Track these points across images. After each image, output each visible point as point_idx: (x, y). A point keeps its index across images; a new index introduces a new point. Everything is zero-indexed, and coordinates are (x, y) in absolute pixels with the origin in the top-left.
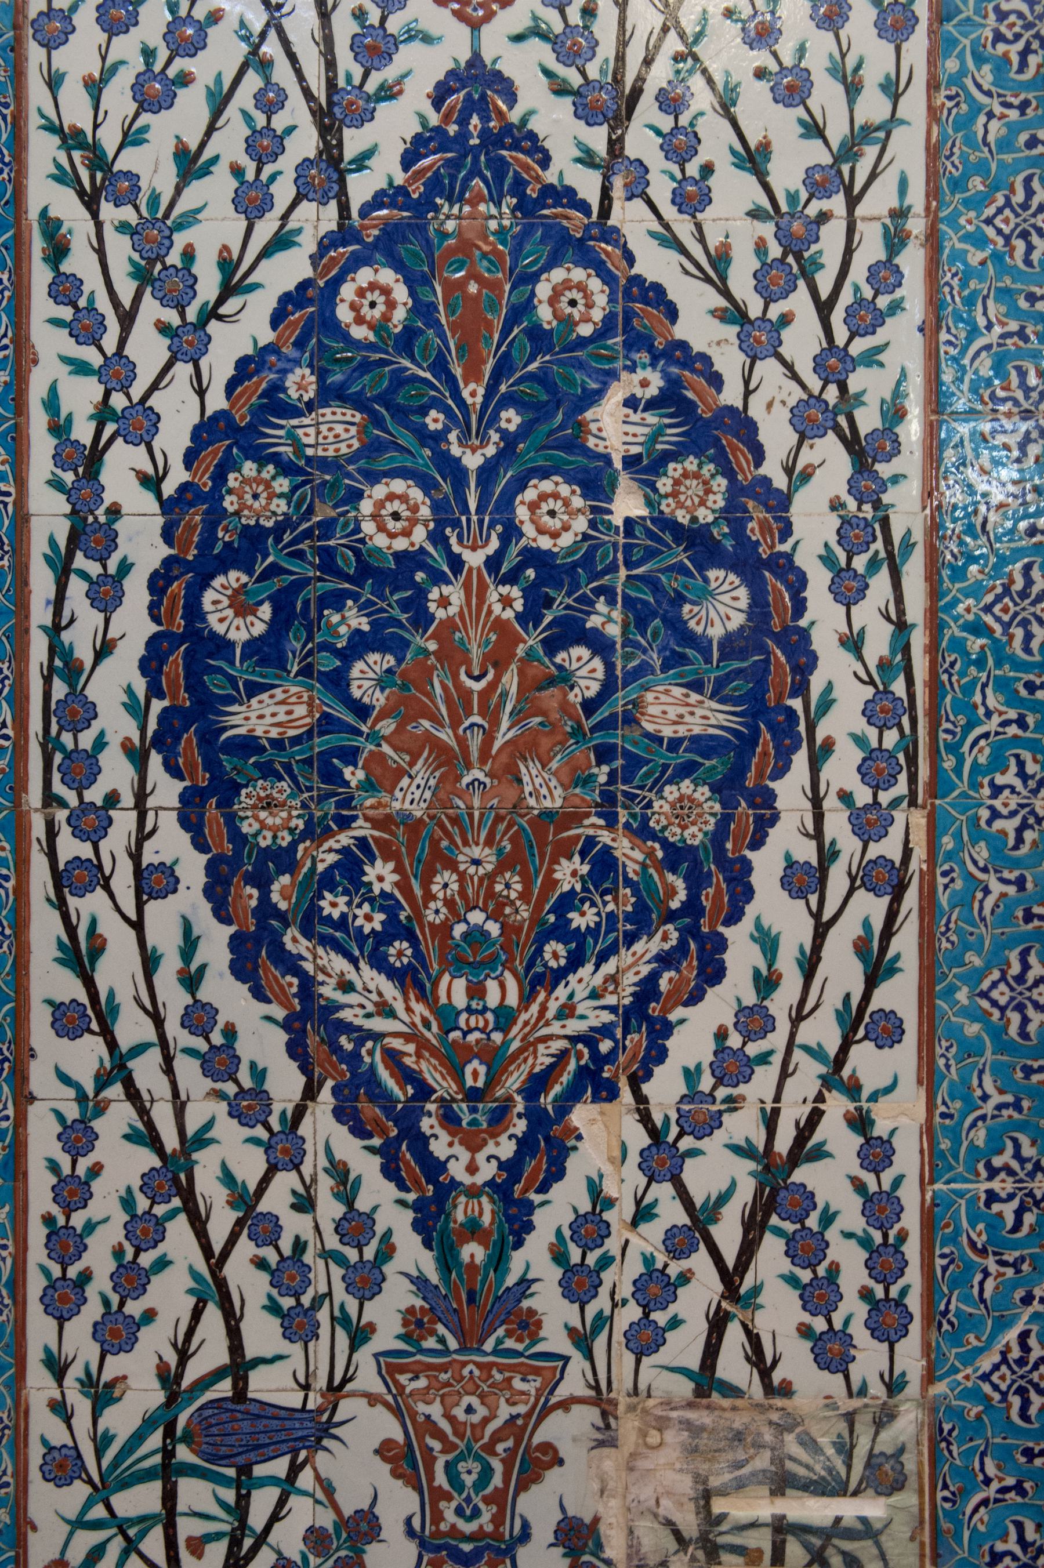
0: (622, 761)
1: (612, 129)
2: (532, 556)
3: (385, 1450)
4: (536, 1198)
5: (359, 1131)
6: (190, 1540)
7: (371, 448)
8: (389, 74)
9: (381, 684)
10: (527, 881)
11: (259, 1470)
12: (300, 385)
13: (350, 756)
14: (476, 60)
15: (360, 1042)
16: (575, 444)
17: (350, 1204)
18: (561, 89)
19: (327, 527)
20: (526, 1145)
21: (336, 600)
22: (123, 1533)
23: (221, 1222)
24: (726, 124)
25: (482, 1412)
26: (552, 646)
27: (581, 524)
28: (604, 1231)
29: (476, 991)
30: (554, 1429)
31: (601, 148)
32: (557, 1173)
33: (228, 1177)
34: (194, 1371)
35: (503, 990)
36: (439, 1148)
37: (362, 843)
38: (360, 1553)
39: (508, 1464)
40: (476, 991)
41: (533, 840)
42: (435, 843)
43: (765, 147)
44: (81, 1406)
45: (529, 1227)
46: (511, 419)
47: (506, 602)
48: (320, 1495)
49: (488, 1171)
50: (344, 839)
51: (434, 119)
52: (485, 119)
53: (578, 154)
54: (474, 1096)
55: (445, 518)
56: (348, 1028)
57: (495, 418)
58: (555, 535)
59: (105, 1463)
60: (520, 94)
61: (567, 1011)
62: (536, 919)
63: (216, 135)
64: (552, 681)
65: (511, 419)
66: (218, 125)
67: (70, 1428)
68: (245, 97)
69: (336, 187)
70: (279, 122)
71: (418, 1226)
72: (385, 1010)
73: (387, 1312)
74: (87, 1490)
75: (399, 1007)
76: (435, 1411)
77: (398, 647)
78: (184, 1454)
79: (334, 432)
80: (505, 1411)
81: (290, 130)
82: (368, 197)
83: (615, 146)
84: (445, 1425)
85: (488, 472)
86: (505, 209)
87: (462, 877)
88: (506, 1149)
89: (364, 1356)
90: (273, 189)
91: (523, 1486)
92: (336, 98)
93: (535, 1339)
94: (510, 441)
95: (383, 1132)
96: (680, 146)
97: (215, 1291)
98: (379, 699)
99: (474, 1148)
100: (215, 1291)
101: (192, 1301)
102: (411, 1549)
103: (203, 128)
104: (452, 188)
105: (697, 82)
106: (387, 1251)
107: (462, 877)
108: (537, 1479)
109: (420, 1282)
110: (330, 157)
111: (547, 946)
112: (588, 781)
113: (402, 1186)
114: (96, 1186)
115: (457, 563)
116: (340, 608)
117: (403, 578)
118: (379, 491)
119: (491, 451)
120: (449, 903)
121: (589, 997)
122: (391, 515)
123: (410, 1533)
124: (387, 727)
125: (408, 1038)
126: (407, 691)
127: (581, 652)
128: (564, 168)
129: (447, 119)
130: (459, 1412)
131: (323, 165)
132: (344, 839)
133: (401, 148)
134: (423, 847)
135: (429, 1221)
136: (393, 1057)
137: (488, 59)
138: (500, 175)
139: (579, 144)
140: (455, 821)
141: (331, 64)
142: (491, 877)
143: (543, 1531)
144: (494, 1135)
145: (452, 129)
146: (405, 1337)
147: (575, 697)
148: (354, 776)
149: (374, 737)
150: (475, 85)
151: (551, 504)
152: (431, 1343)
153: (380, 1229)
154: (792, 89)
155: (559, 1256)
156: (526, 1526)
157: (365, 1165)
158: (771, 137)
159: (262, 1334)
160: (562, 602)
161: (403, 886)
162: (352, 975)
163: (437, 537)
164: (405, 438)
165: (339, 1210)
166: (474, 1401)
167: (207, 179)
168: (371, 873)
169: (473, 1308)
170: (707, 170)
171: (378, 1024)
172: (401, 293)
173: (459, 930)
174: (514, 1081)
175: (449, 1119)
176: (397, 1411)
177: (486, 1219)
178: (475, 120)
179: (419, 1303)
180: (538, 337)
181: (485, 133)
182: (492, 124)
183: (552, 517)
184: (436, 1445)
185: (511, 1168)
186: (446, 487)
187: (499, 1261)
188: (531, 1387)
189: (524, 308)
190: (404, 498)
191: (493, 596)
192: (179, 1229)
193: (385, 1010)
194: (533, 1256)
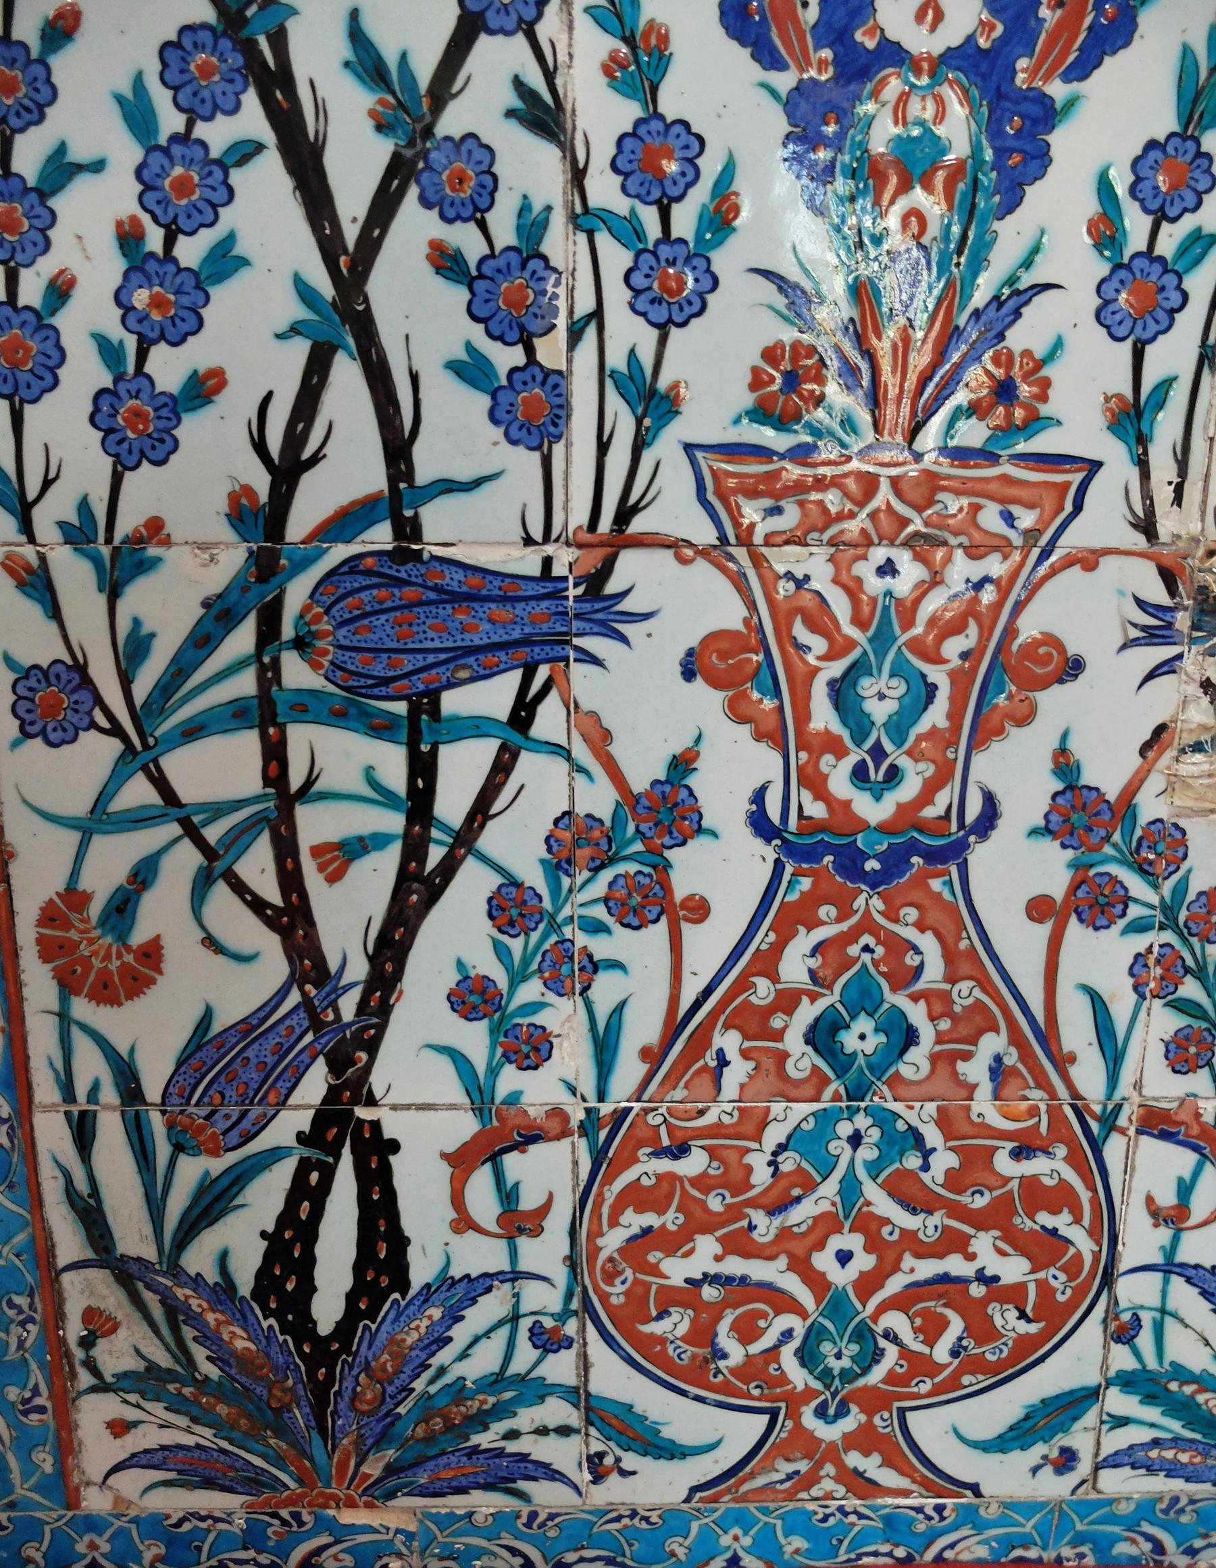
6: (317, 851)
11: (454, 702)
22: (192, 832)
23: (356, 162)
33: (368, 64)
34: (312, 503)
38: (663, 868)
44: (74, 575)
48: (581, 752)
59: (142, 689)
67: (55, 612)
74: (114, 746)
78: (297, 673)
91: (984, 733)
97: (343, 321)
100: (343, 321)
101: (300, 349)
114: (64, 66)
123: (760, 824)
159: (456, 430)
192: (266, 187)
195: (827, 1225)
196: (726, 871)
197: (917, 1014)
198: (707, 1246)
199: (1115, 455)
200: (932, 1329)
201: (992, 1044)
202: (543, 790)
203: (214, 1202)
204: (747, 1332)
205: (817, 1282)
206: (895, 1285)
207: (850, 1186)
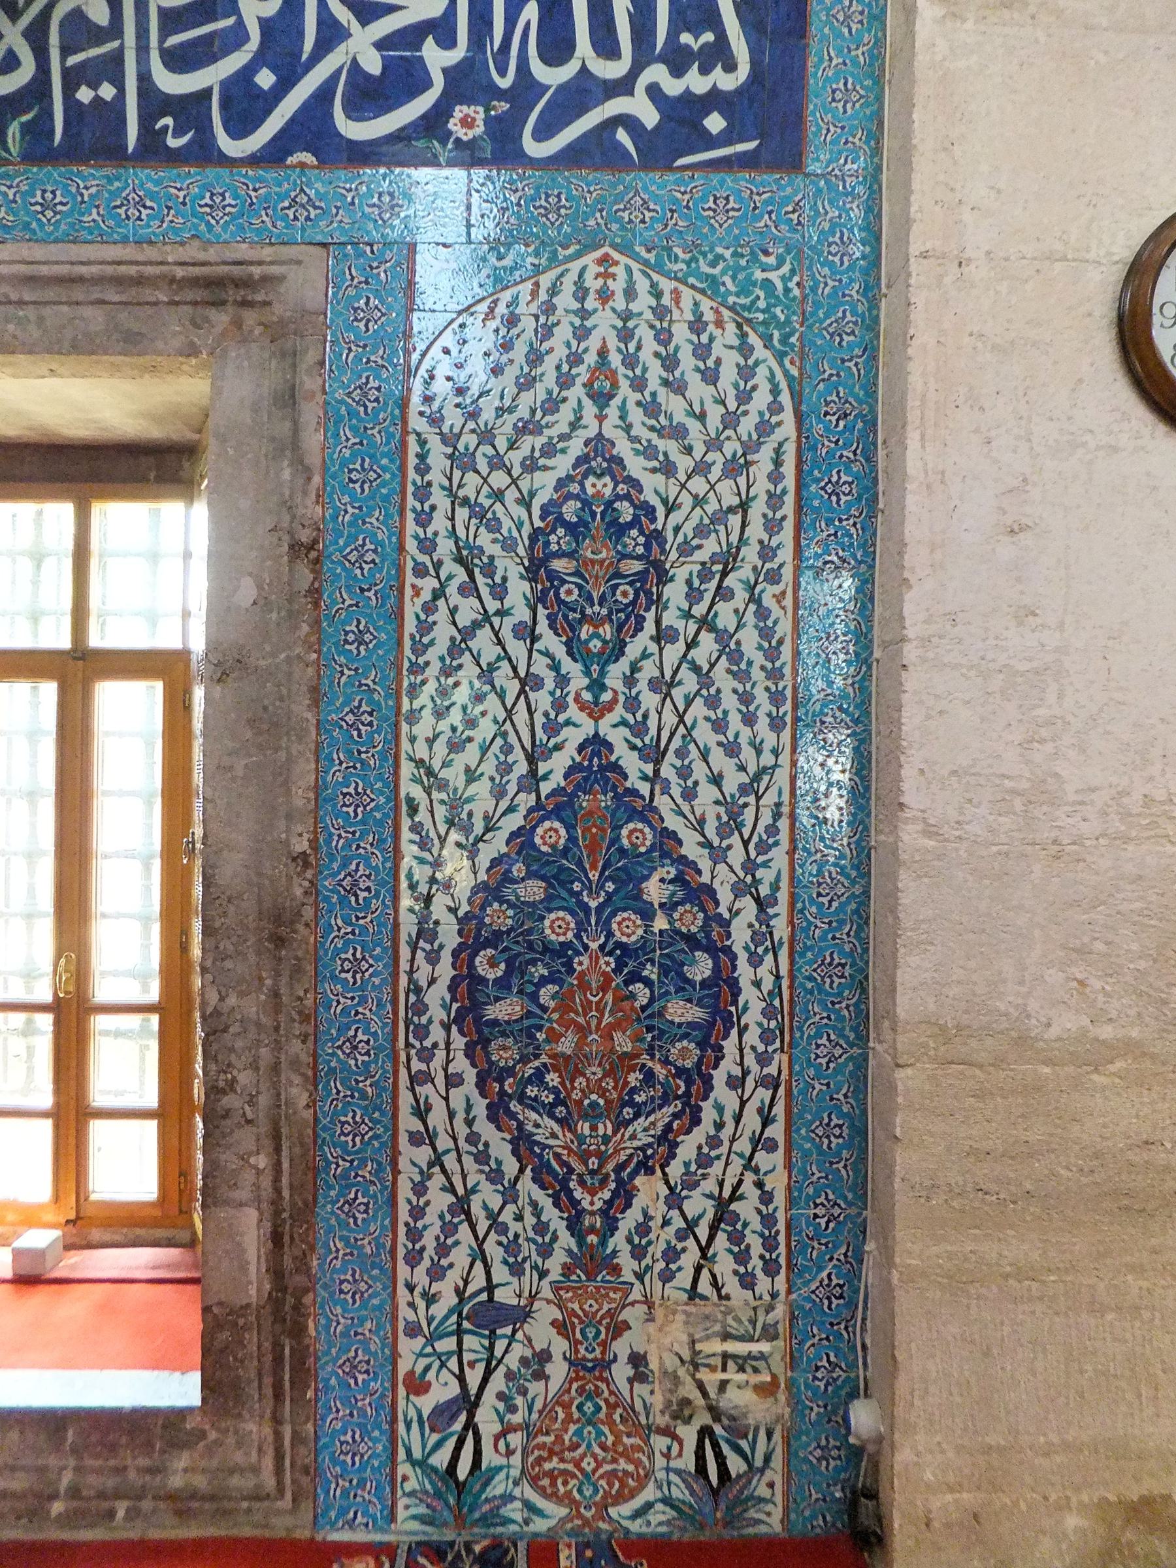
0: (656, 1030)
2: (619, 945)
3: (554, 1323)
4: (619, 1216)
5: (543, 1187)
7: (549, 898)
9: (553, 998)
10: (616, 1082)
12: (518, 870)
13: (540, 1028)
15: (543, 1150)
16: (638, 896)
17: (539, 1218)
19: (530, 932)
20: (615, 1194)
21: (533, 962)
25: (596, 1307)
26: (627, 983)
27: (640, 932)
28: (648, 1230)
29: (594, 1128)
30: (625, 1315)
32: (628, 1205)
35: (606, 1127)
36: (578, 1194)
37: (544, 1065)
39: (608, 1329)
40: (594, 1128)
41: (619, 1064)
42: (576, 1065)
45: (617, 1228)
46: (610, 887)
47: (608, 964)
49: (599, 1205)
50: (537, 1063)
54: (593, 1173)
55: (581, 928)
56: (538, 1143)
57: (603, 887)
58: (629, 936)
61: (633, 1137)
62: (620, 1098)
64: (627, 998)
65: (610, 887)
71: (568, 1228)
72: (554, 1136)
73: (555, 1264)
75: (560, 1135)
76: (576, 1306)
77: (560, 982)
79: (533, 890)
80: (606, 1307)
84: (580, 1313)
85: (600, 909)
87: (588, 1080)
88: (607, 1195)
89: (545, 1283)
91: (614, 1338)
93: (619, 1276)
94: (609, 896)
95: (553, 1188)
98: (552, 1004)
99: (593, 1194)
102: (566, 1366)
106: (555, 1238)
107: (588, 1080)
108: (620, 1335)
109: (569, 1252)
111: (623, 1110)
112: (643, 1040)
113: (561, 1211)
115: (586, 947)
116: (535, 965)
117: (562, 953)
118: (553, 916)
119: (601, 900)
120: (582, 1091)
121: (642, 1132)
122: (557, 926)
123: (565, 1358)
124: (555, 1016)
125: (564, 1148)
126: (565, 1005)
127: (640, 985)
130: (586, 1307)
132: (537, 1063)
134: (570, 1066)
135: (574, 1226)
136: (557, 1156)
138: (606, 783)
140: (585, 1056)
142: (601, 1080)
143: (623, 1357)
144: (602, 1189)
146: (563, 1275)
147: (637, 1005)
148: (541, 1036)
149: (550, 1020)
151: (627, 923)
152: (574, 1277)
153: (552, 1229)
154: (732, 749)
155: (629, 1240)
156: (615, 1356)
157: (546, 1202)
160: (631, 964)
161: (562, 1083)
162: (540, 1121)
163: (578, 936)
164: (564, 894)
165: (534, 1221)
166: (592, 1302)
168: (548, 1078)
169: (593, 1262)
171: (551, 1142)
172: (563, 832)
173: (586, 1102)
174: (610, 1166)
175: (582, 1182)
176: (560, 1308)
177: (598, 1225)
179: (569, 1260)
180: (622, 851)
183: (628, 928)
184: (576, 1321)
185: (609, 1203)
186: (582, 915)
187: (603, 1243)
188: (618, 1296)
189: (616, 839)
190: (563, 919)
191: (602, 962)
193: (554, 1136)
194: (618, 1241)
195: (584, 1455)
196: (558, 1370)
197: (602, 1404)
198: (555, 1459)
199: (637, 1283)
200: (611, 1485)
201: (619, 1411)
202: (518, 1350)
203: (438, 1445)
204: (565, 1483)
205: (582, 1470)
206: (601, 1471)
207: (589, 1446)
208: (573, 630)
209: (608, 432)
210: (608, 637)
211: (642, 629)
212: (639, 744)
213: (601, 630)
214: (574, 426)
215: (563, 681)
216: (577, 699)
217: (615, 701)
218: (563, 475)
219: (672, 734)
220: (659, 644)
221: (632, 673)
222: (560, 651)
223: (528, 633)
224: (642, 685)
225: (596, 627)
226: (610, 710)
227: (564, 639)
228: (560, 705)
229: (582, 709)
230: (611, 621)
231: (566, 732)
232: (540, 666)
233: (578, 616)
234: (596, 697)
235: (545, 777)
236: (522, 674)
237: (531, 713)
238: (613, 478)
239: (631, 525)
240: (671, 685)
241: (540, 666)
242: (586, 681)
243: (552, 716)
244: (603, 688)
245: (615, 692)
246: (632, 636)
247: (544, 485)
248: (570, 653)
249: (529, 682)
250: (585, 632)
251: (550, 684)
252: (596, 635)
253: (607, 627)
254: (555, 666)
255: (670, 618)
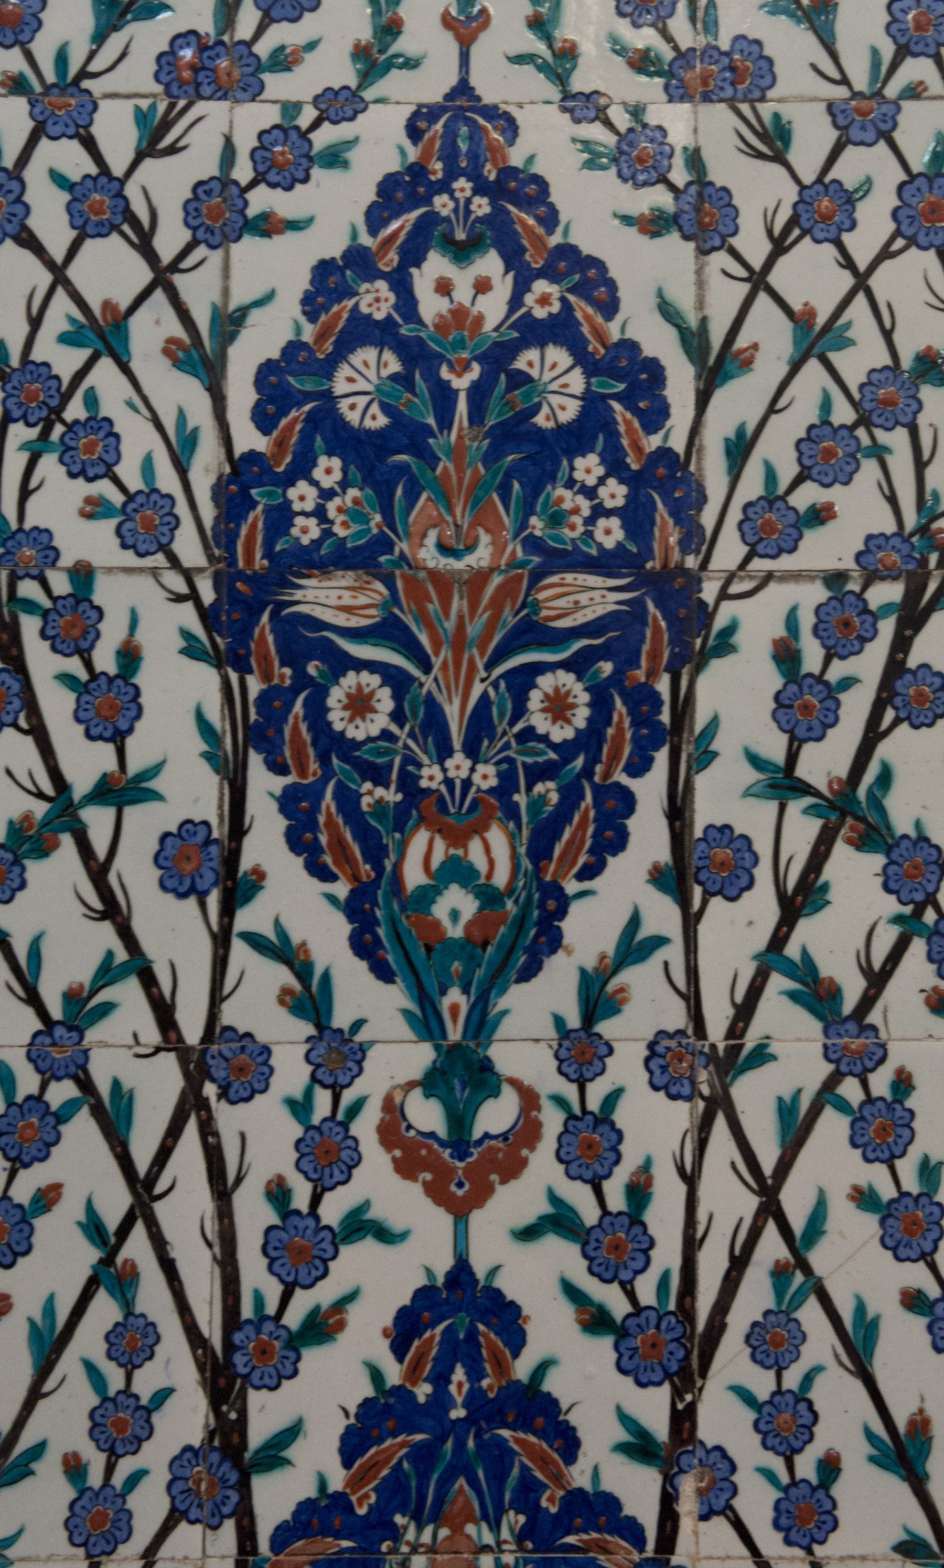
1: (677, 1394)
8: (324, 1294)
14: (461, 1271)
18: (596, 1320)
24: (857, 1387)
31: (659, 1425)
43: (921, 1426)
51: (394, 1374)
52: (475, 1374)
53: (623, 1436)
60: (531, 1330)
63: (42, 1406)
66: (47, 1388)
68: (89, 1340)
69: (234, 1497)
70: (146, 1383)
81: (163, 1396)
82: (285, 1513)
83: (683, 1419)
86: (505, 1534)
90: (134, 1501)
92: (238, 1337)
96: (786, 1421)
103: (21, 1394)
104: (422, 1498)
105: (811, 1315)
110: (225, 1437)
128: (602, 1465)
129: (413, 1374)
131: (215, 1457)
133: (340, 1425)
137: (480, 1269)
138: (498, 1478)
139: (624, 1419)
141: (228, 1264)
145: (423, 1391)
150: (459, 1313)
158: (931, 1411)
167: (26, 1485)
170: (830, 1467)
178: (459, 1374)
181: (474, 1399)
182: (485, 1383)
208: (375, 852)
209: (494, 82)
210: (501, 878)
211: (619, 842)
212: (619, 1306)
213: (475, 853)
214: (374, 60)
215: (338, 1054)
216: (393, 1128)
217: (526, 1131)
218: (335, 249)
219: (739, 1263)
220: (684, 902)
221: (590, 1016)
222: (326, 935)
223: (210, 868)
224: (626, 1067)
225: (458, 838)
226: (512, 1169)
227: (341, 889)
228: (327, 1155)
229: (405, 1169)
230: (512, 813)
231: (354, 1264)
232: (257, 1001)
233: (392, 796)
234: (460, 1121)
235: (274, 1455)
236: (192, 1029)
237: (222, 1187)
238: (513, 258)
239: (575, 438)
240: (735, 1060)
241: (257, 1001)
242: (420, 1057)
243: (301, 1199)
244: (482, 1079)
245: (529, 1099)
246: (591, 872)
247: (268, 284)
248: (363, 945)
249: (219, 1066)
250: (418, 856)
251: (291, 1071)
252: (457, 872)
253: (497, 837)
254: (310, 998)
255: (723, 797)
